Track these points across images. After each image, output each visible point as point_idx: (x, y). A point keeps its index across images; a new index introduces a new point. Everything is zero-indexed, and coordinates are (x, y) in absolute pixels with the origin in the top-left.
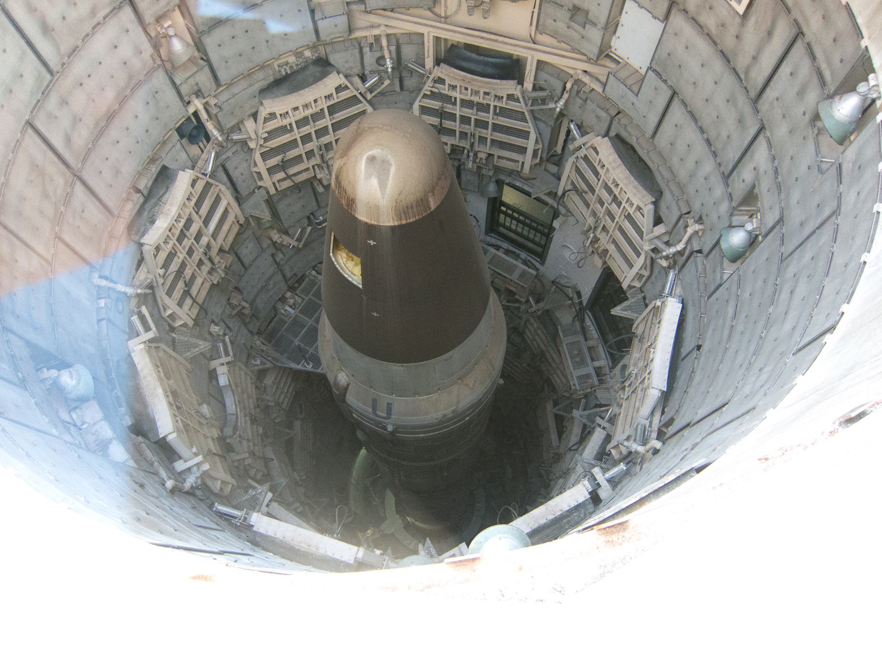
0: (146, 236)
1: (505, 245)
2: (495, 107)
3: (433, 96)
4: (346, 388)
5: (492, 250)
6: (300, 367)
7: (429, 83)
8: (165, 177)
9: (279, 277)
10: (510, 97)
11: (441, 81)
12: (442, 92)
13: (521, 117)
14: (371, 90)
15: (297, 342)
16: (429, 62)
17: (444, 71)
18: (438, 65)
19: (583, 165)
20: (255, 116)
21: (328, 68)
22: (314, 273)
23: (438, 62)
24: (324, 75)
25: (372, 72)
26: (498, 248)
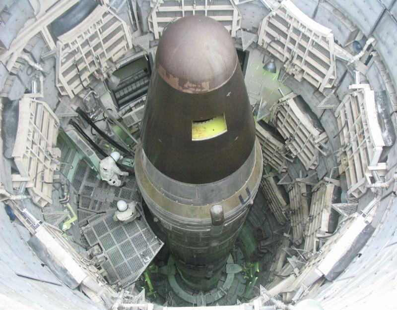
0: (76, 279)
1: (132, 104)
2: (99, 30)
3: (68, 58)
4: (222, 213)
5: (131, 113)
6: (145, 266)
7: (62, 53)
8: (35, 246)
9: (81, 248)
10: (105, 14)
11: (67, 45)
12: (70, 51)
13: (115, 19)
14: (39, 91)
15: (126, 261)
16: (51, 44)
17: (64, 38)
18: (58, 40)
19: (162, 9)
20: (15, 170)
21: (15, 104)
22: (83, 228)
23: (56, 40)
24: (17, 110)
25: (30, 82)
26: (131, 110)
